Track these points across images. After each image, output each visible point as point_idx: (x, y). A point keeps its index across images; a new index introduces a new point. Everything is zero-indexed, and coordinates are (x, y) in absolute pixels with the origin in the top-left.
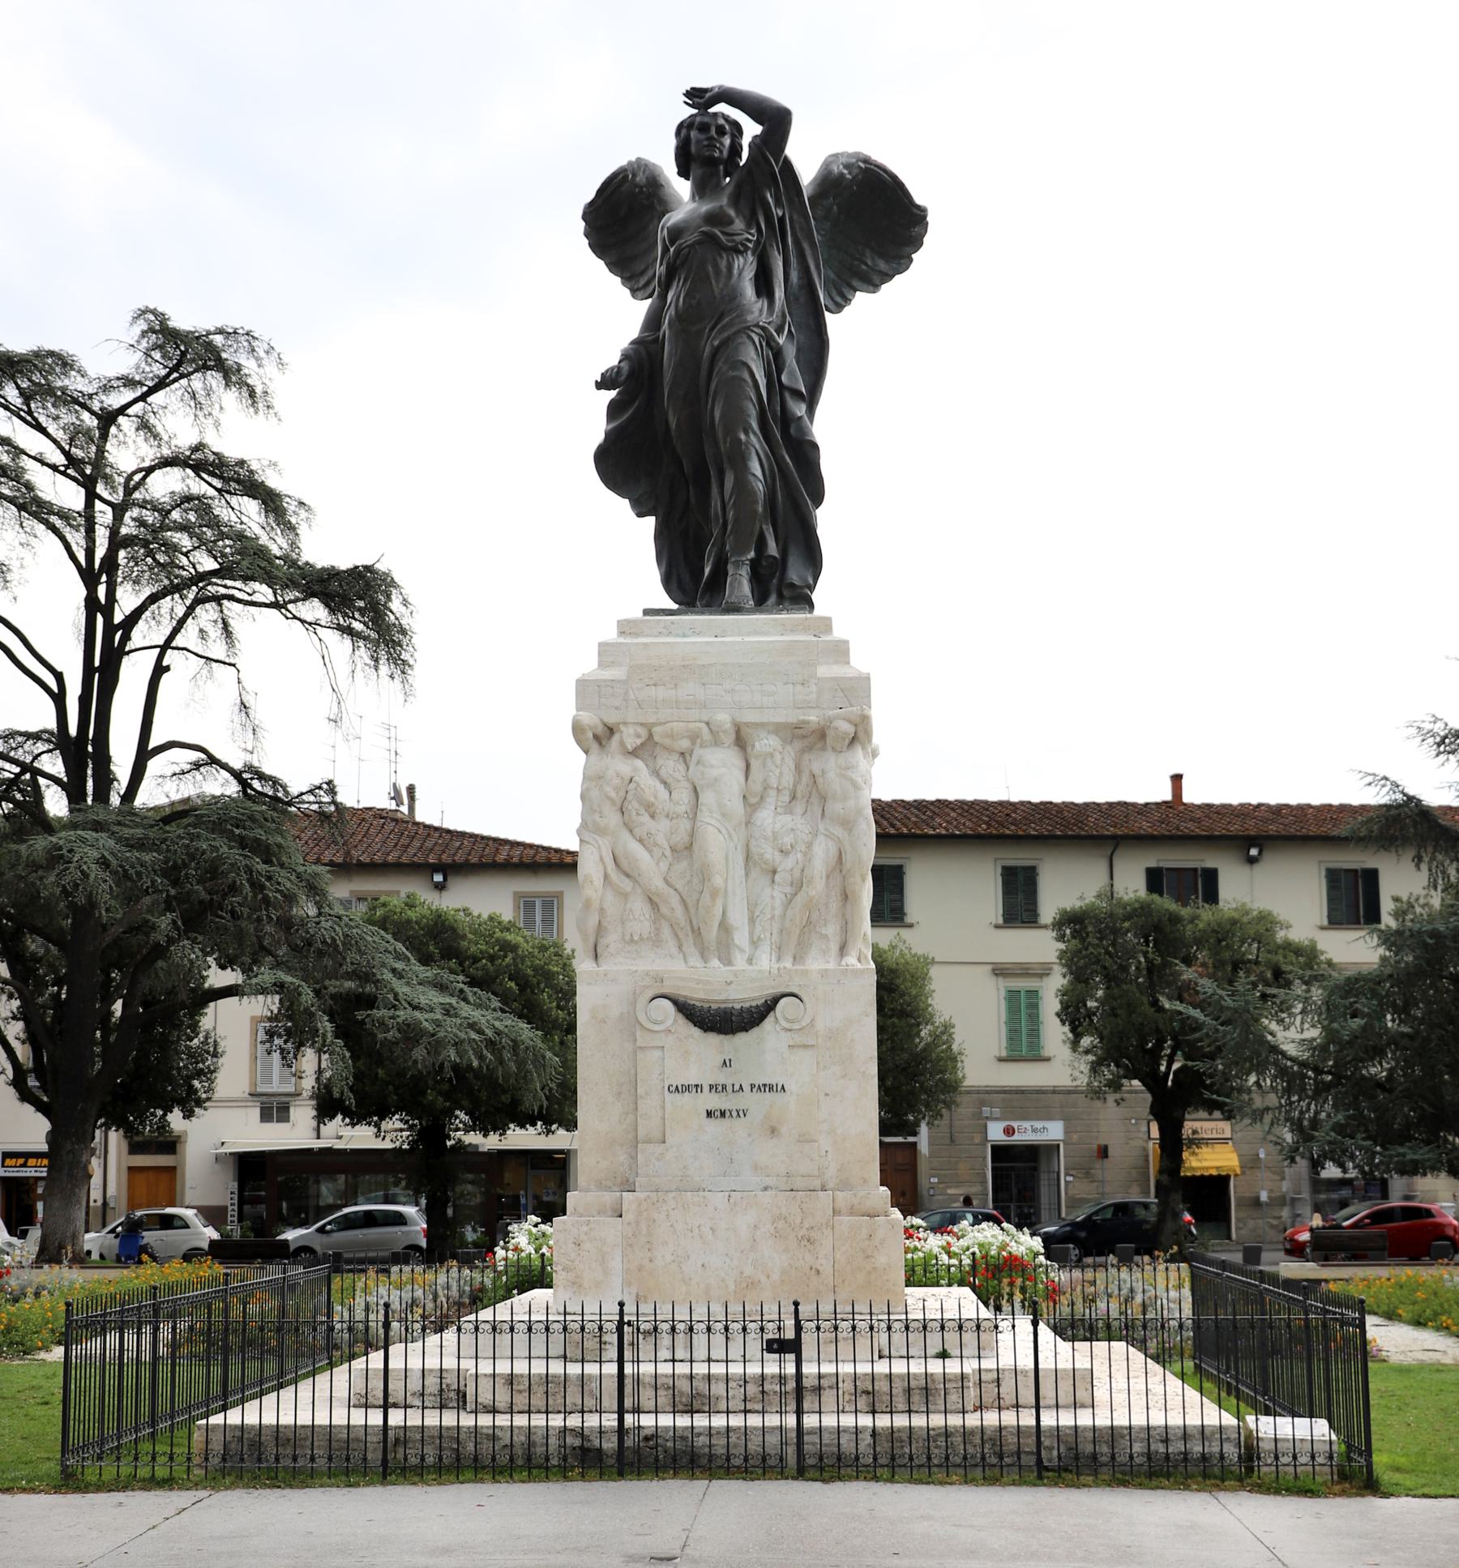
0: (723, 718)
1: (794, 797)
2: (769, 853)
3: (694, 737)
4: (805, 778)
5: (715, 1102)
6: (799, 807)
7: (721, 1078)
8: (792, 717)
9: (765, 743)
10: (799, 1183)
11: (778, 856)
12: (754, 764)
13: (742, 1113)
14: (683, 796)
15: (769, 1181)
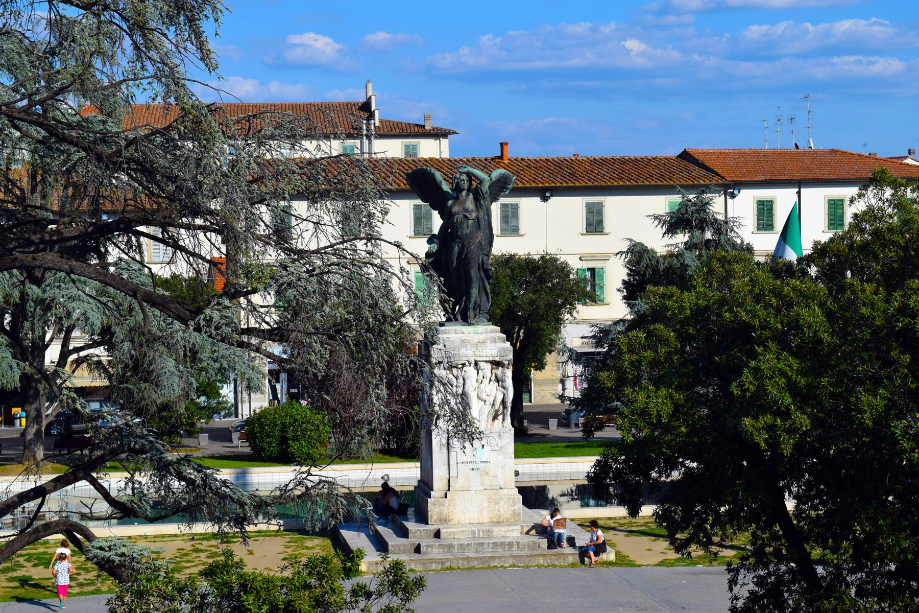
0: (472, 360)
1: (490, 380)
2: (484, 397)
3: (464, 365)
4: (494, 375)
5: (471, 466)
6: (492, 382)
7: (473, 459)
8: (491, 359)
9: (482, 365)
10: (494, 488)
11: (487, 397)
12: (480, 371)
13: (478, 469)
14: (461, 381)
15: (486, 488)
